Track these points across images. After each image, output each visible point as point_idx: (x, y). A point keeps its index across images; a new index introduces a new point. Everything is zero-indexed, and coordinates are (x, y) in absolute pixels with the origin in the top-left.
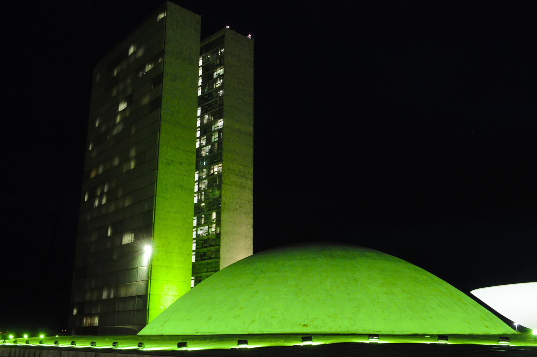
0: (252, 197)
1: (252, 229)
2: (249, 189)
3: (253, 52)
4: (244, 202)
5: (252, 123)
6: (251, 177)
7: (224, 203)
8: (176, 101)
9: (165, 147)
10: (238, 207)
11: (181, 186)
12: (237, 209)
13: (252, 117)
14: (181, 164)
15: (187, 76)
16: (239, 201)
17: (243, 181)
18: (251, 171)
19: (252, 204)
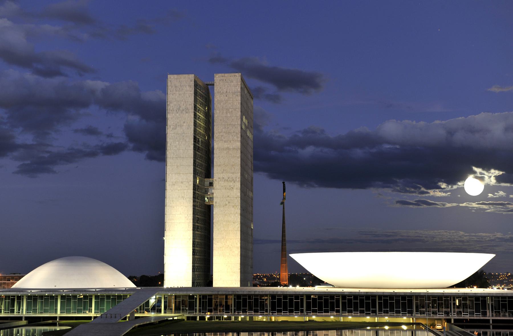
0: (239, 194)
1: (240, 217)
2: (237, 189)
3: (240, 84)
4: (232, 198)
5: (239, 139)
6: (239, 180)
7: (216, 202)
8: (177, 143)
9: (171, 175)
10: (227, 203)
11: (183, 197)
12: (226, 205)
13: (239, 136)
14: (182, 183)
15: (184, 122)
16: (228, 199)
17: (232, 184)
18: (239, 175)
19: (240, 199)
